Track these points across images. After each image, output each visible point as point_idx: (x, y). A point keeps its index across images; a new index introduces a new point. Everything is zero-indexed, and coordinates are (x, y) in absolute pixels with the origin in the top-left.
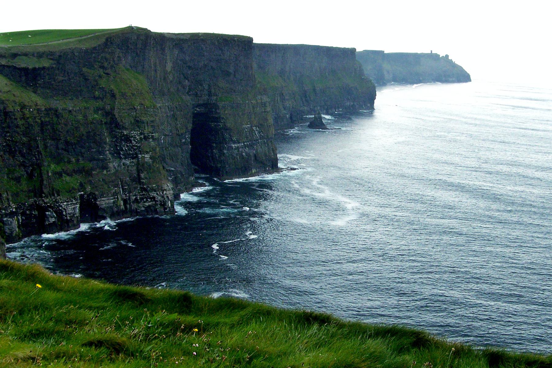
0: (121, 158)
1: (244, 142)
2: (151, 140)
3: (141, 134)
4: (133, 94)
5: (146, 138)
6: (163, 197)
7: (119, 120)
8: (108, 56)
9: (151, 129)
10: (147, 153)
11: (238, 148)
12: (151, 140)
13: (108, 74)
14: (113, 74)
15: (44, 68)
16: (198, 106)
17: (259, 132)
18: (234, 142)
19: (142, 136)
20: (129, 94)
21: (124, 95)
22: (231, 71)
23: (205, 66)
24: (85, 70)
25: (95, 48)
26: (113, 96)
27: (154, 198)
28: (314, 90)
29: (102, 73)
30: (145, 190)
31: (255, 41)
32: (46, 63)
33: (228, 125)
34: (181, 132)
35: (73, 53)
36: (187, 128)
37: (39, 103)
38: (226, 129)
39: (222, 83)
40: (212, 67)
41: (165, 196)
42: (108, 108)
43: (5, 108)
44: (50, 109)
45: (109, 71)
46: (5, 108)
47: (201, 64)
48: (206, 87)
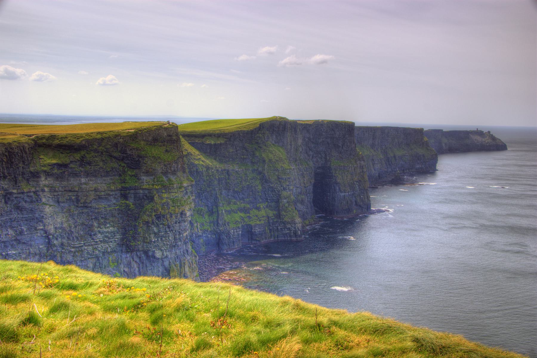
0: (268, 202)
3: (281, 186)
4: (277, 161)
7: (267, 177)
8: (261, 135)
15: (221, 144)
18: (342, 192)
19: (282, 188)
21: (270, 160)
27: (289, 228)
28: (395, 157)
29: (257, 147)
30: (284, 223)
32: (221, 141)
35: (239, 134)
36: (311, 182)
37: (217, 166)
38: (336, 183)
42: (260, 169)
43: (197, 169)
44: (225, 170)
46: (197, 169)
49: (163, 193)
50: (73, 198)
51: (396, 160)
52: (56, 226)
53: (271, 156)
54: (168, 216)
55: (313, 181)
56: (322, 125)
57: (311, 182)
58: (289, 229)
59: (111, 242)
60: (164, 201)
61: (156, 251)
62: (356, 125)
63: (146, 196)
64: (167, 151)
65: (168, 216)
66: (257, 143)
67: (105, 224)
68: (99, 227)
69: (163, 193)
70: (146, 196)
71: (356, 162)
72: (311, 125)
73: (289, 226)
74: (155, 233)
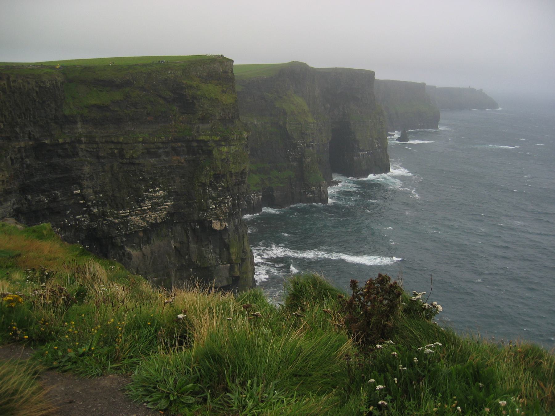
0: (289, 161)
1: (367, 151)
2: (311, 148)
3: (304, 143)
5: (308, 146)
6: (320, 191)
9: (311, 140)
10: (309, 157)
12: (311, 148)
17: (378, 144)
18: (361, 151)
27: (313, 191)
36: (328, 139)
41: (322, 190)
50: (116, 151)
52: (95, 189)
54: (228, 176)
55: (330, 138)
57: (328, 139)
58: (313, 192)
59: (161, 210)
60: (224, 157)
61: (213, 222)
62: (377, 77)
65: (228, 176)
67: (153, 186)
68: (147, 191)
73: (313, 189)
74: (214, 199)
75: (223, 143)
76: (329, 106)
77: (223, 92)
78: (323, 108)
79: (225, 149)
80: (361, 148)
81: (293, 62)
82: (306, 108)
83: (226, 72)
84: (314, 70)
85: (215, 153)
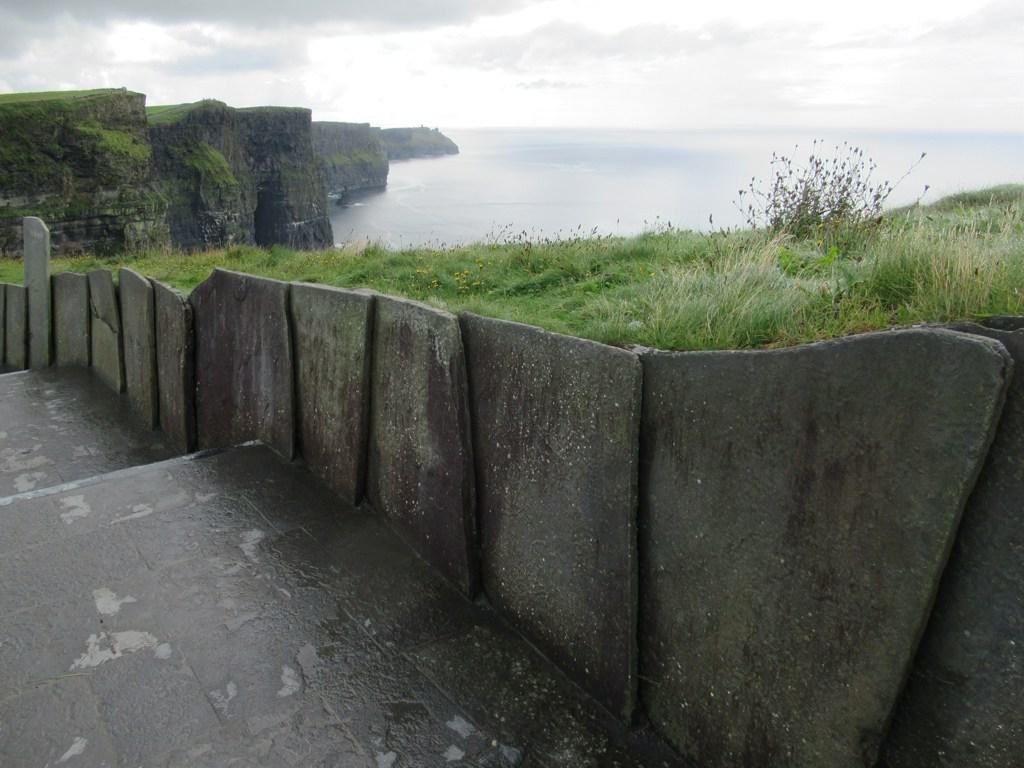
4: (217, 173)
7: (204, 201)
8: (191, 132)
11: (299, 226)
13: (191, 152)
14: (197, 152)
16: (262, 184)
20: (213, 172)
21: (208, 173)
22: (292, 145)
23: (270, 141)
24: (170, 147)
25: (178, 124)
26: (197, 174)
28: (334, 167)
31: (316, 117)
33: (291, 203)
34: (248, 212)
35: (159, 129)
38: (288, 207)
39: (284, 159)
40: (275, 142)
45: (192, 148)
47: (266, 139)
48: (269, 163)
49: (136, 221)
51: (335, 172)
53: (208, 165)
55: (256, 206)
56: (268, 114)
62: (316, 118)
63: (107, 229)
64: (134, 142)
66: (186, 144)
69: (136, 221)
70: (107, 229)
71: (313, 172)
72: (252, 115)
75: (138, 218)
76: (252, 160)
77: (134, 142)
78: (245, 164)
79: (140, 226)
80: (296, 217)
81: (204, 101)
82: (226, 165)
83: (135, 113)
84: (232, 109)
85: (127, 231)
